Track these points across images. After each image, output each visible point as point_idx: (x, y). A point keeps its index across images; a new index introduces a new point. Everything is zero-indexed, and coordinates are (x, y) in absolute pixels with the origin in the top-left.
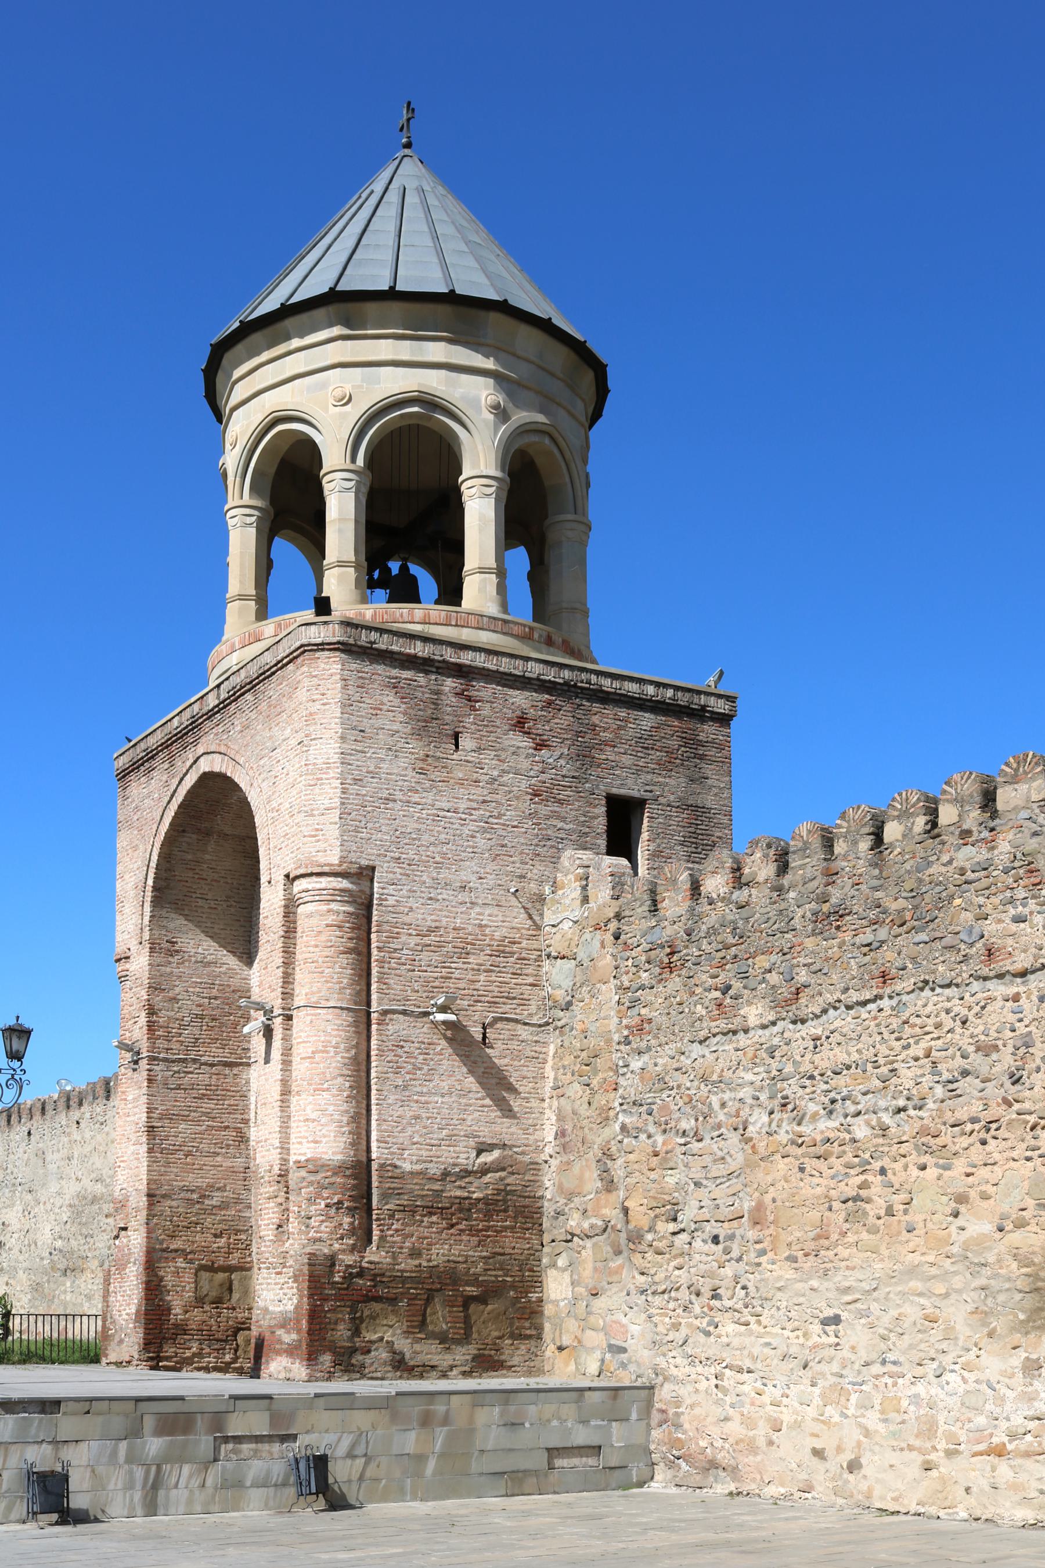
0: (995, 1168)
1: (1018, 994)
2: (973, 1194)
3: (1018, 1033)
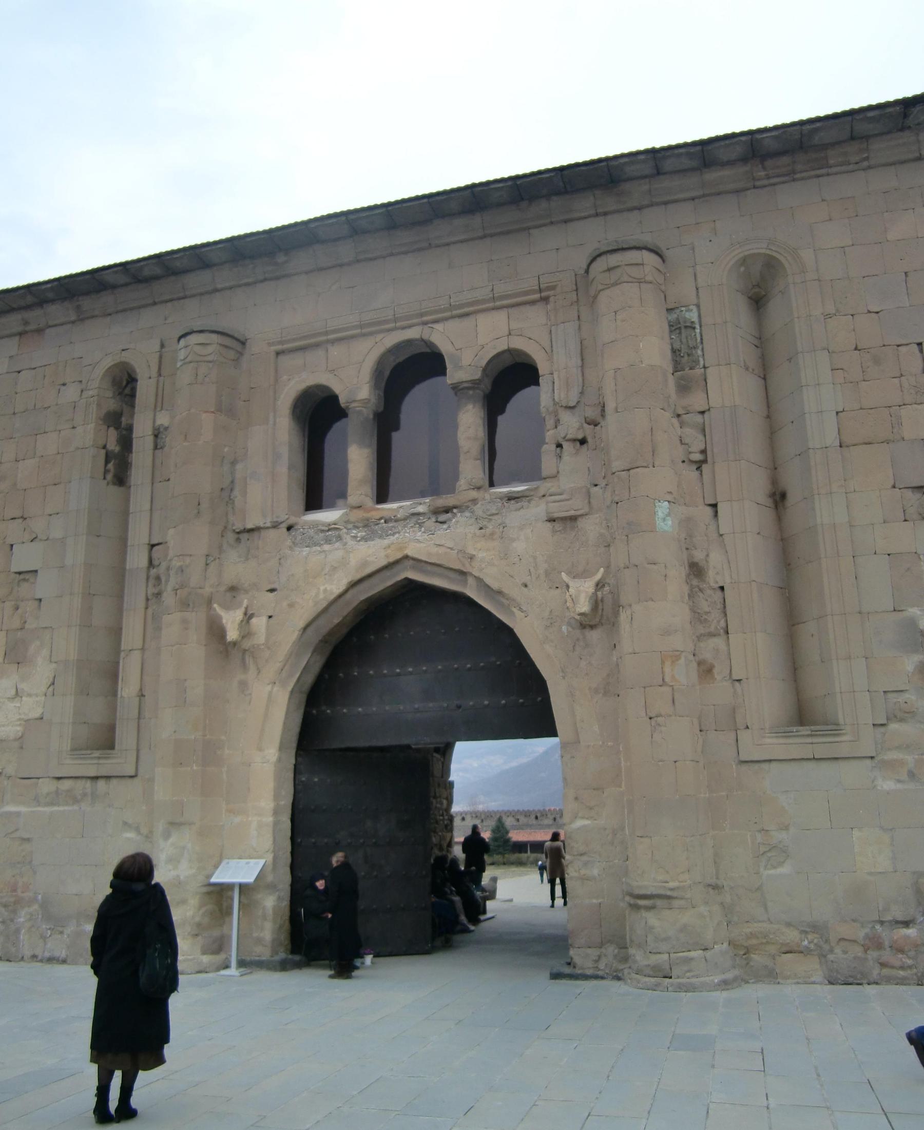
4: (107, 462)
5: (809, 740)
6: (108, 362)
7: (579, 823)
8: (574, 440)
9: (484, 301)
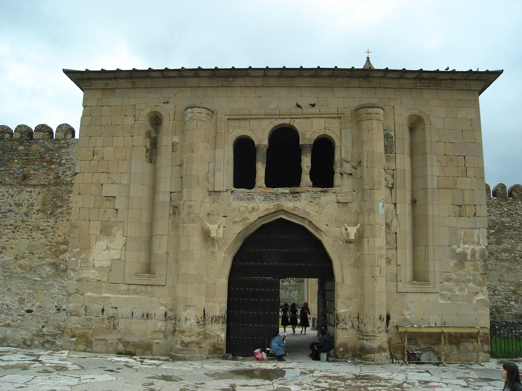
0: (16, 240)
1: (32, 191)
2: (8, 247)
3: (30, 202)
4: (147, 153)
5: (420, 286)
6: (148, 110)
9: (316, 114)
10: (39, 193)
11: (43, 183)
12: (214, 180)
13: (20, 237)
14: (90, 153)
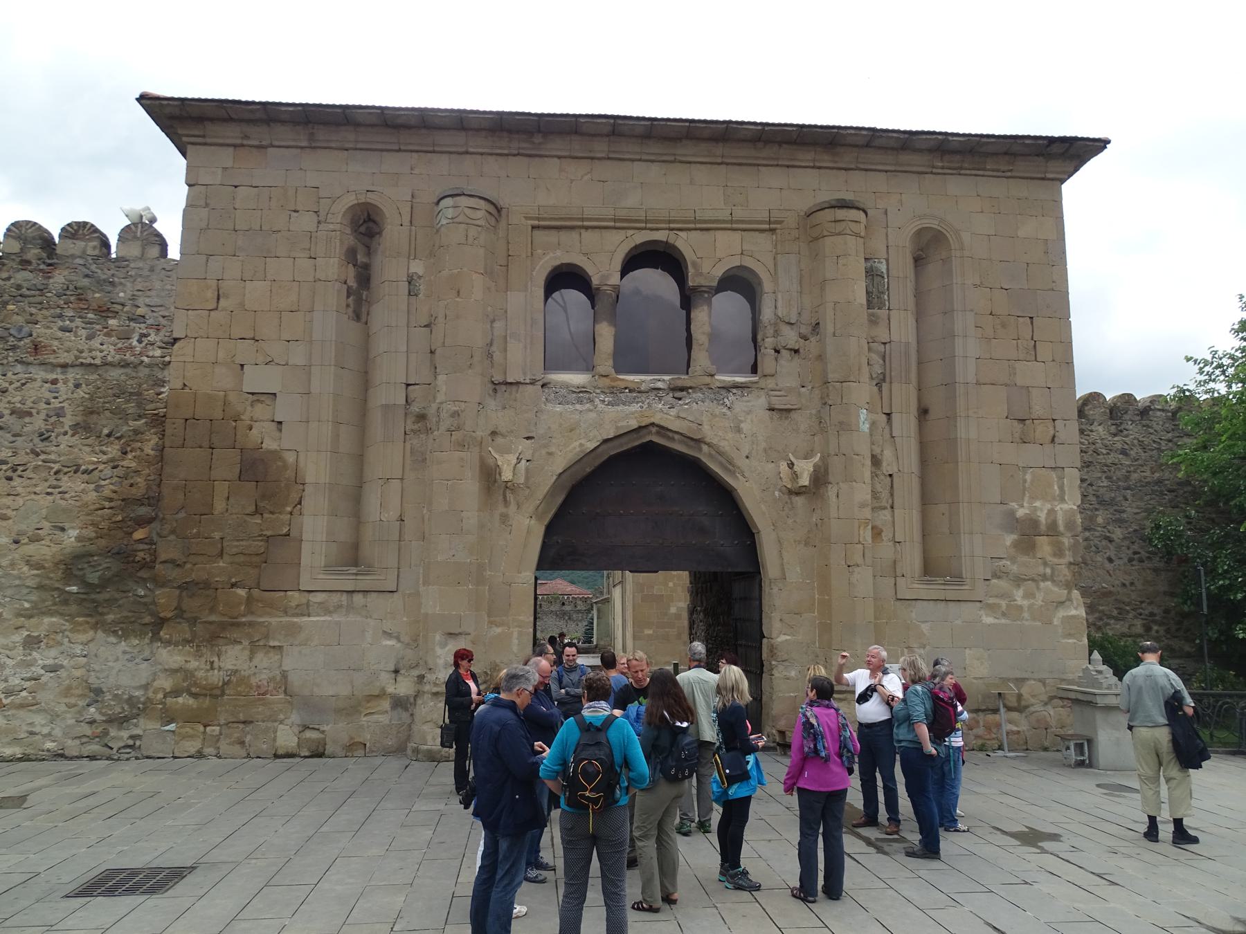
0: (17, 498)
1: (56, 379)
3: (52, 406)
4: (348, 297)
5: (943, 587)
6: (351, 200)
7: (783, 638)
8: (791, 350)
10: (77, 386)
11: (89, 361)
12: (506, 359)
13: (28, 490)
14: (211, 294)
